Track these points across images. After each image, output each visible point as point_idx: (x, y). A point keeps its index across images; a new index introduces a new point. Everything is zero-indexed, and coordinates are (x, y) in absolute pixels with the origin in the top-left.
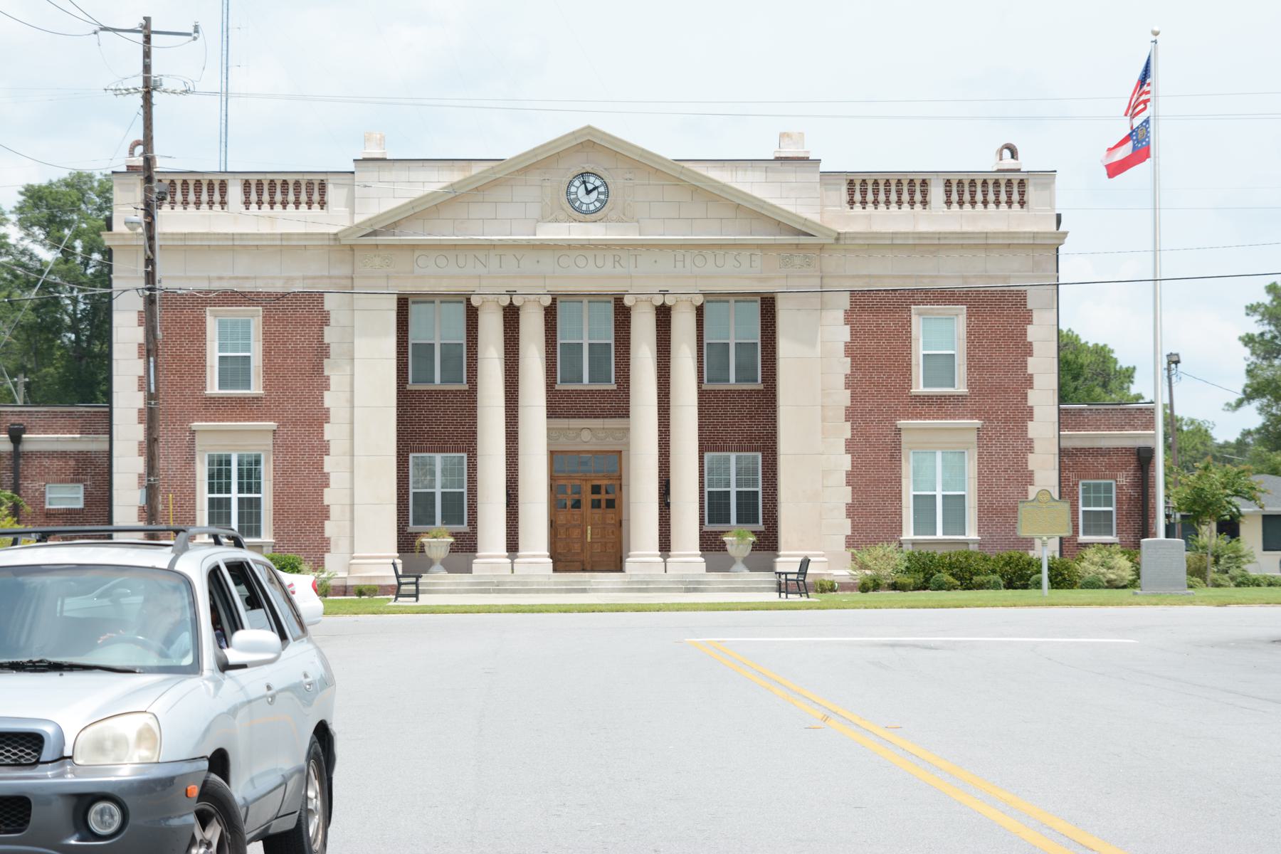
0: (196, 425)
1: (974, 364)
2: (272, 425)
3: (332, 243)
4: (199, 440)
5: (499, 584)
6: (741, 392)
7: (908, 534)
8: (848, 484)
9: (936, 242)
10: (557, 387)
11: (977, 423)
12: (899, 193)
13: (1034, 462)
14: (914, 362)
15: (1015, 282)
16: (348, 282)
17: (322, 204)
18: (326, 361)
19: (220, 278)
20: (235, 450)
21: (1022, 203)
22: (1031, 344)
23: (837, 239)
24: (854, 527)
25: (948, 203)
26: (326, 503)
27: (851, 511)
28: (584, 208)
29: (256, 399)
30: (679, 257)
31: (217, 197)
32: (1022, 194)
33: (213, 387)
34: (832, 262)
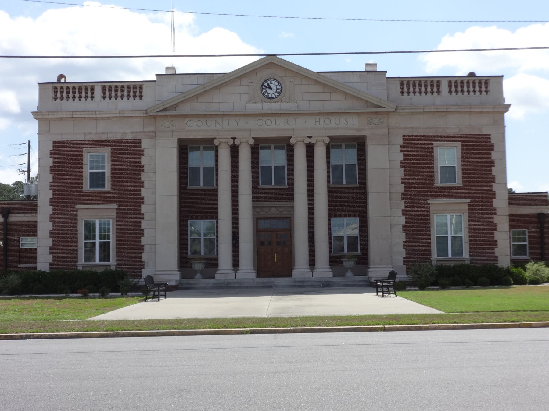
0: (77, 207)
1: (465, 172)
2: (116, 206)
3: (145, 115)
4: (80, 213)
5: (228, 283)
6: (348, 188)
7: (434, 256)
8: (404, 231)
9: (445, 110)
10: (259, 187)
11: (468, 201)
12: (426, 87)
13: (497, 219)
14: (435, 170)
15: (485, 131)
16: (153, 134)
17: (141, 97)
18: (142, 173)
19: (90, 133)
20: (97, 218)
21: (487, 92)
22: (493, 160)
23: (396, 109)
24: (407, 253)
25: (450, 92)
26: (142, 244)
28: (270, 96)
30: (317, 120)
31: (89, 94)
32: (486, 86)
33: (87, 187)
34: (394, 121)
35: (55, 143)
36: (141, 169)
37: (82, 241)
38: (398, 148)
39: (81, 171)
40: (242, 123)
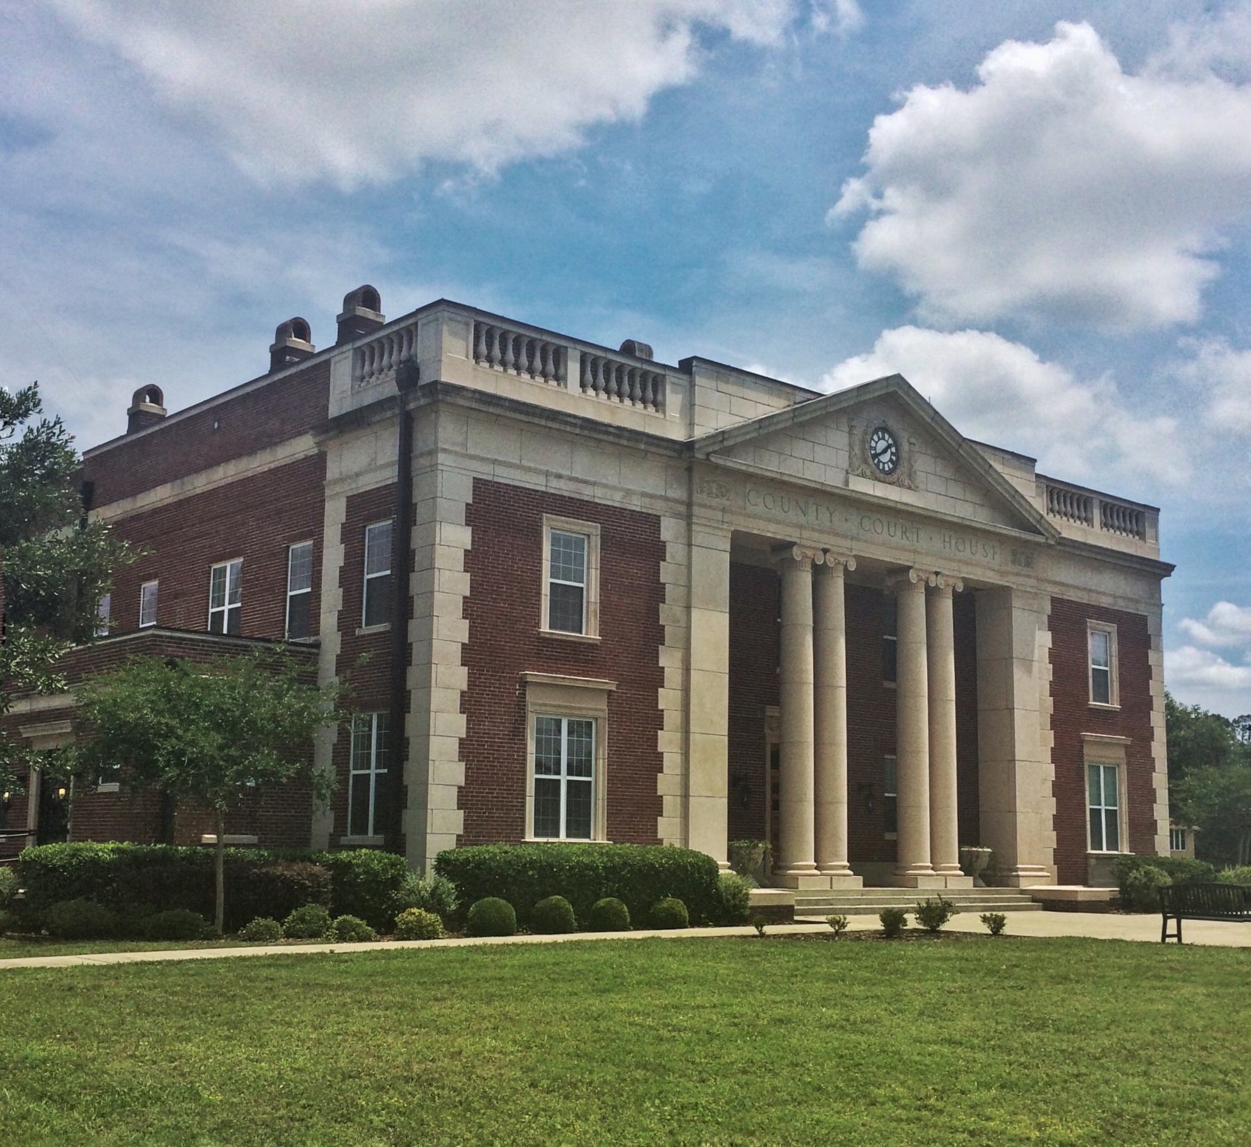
16: (682, 509)
24: (1059, 840)
29: (592, 646)
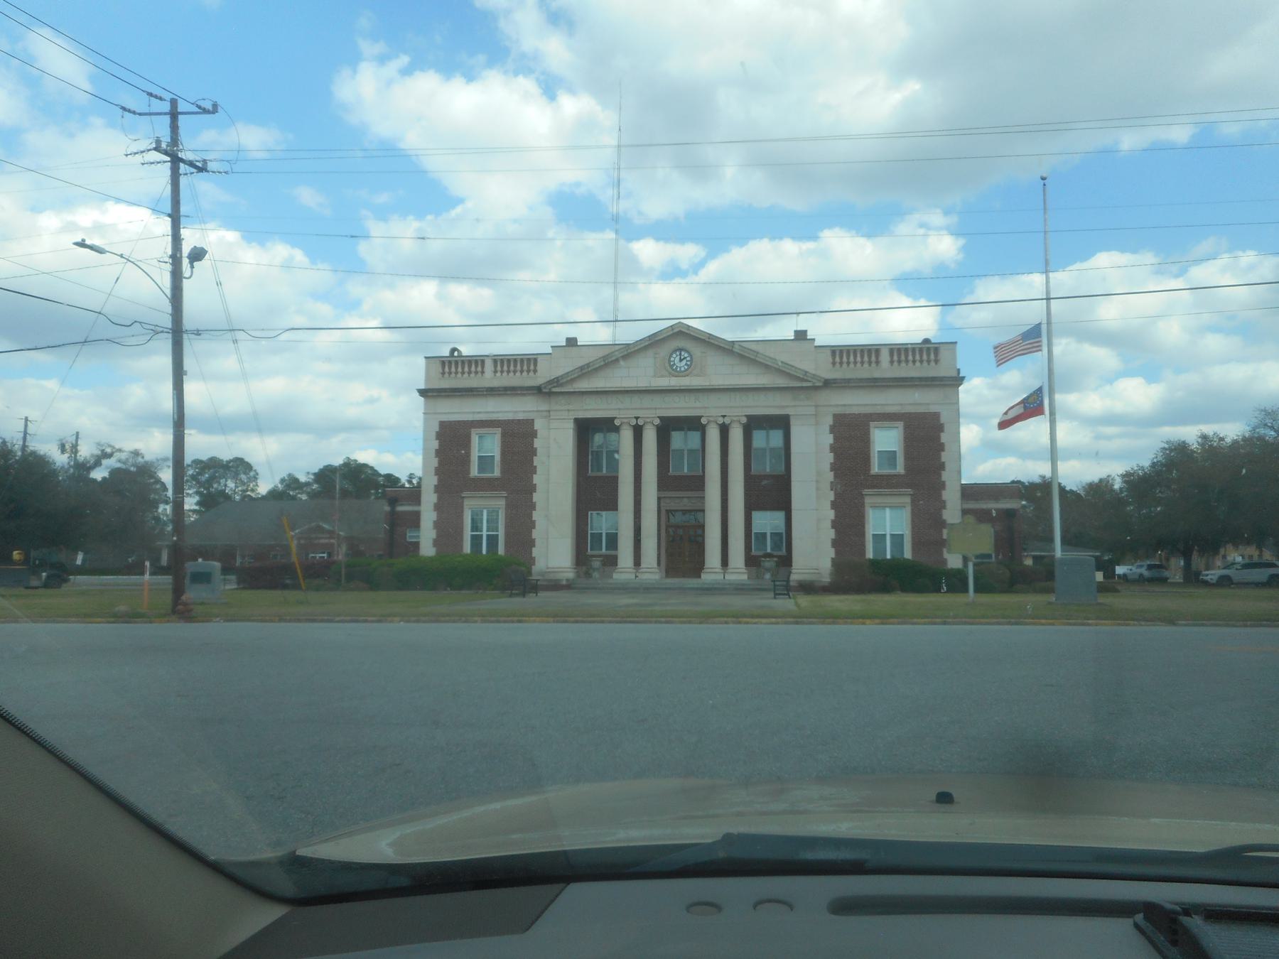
15: (933, 409)
27: (835, 543)
33: (474, 472)
35: (442, 424)
36: (533, 452)
37: (468, 533)
38: (828, 429)
39: (468, 455)
40: (647, 401)
